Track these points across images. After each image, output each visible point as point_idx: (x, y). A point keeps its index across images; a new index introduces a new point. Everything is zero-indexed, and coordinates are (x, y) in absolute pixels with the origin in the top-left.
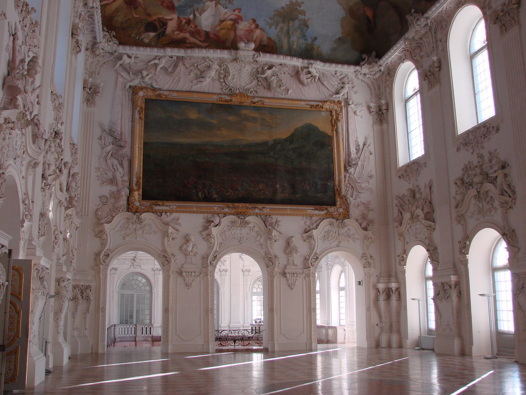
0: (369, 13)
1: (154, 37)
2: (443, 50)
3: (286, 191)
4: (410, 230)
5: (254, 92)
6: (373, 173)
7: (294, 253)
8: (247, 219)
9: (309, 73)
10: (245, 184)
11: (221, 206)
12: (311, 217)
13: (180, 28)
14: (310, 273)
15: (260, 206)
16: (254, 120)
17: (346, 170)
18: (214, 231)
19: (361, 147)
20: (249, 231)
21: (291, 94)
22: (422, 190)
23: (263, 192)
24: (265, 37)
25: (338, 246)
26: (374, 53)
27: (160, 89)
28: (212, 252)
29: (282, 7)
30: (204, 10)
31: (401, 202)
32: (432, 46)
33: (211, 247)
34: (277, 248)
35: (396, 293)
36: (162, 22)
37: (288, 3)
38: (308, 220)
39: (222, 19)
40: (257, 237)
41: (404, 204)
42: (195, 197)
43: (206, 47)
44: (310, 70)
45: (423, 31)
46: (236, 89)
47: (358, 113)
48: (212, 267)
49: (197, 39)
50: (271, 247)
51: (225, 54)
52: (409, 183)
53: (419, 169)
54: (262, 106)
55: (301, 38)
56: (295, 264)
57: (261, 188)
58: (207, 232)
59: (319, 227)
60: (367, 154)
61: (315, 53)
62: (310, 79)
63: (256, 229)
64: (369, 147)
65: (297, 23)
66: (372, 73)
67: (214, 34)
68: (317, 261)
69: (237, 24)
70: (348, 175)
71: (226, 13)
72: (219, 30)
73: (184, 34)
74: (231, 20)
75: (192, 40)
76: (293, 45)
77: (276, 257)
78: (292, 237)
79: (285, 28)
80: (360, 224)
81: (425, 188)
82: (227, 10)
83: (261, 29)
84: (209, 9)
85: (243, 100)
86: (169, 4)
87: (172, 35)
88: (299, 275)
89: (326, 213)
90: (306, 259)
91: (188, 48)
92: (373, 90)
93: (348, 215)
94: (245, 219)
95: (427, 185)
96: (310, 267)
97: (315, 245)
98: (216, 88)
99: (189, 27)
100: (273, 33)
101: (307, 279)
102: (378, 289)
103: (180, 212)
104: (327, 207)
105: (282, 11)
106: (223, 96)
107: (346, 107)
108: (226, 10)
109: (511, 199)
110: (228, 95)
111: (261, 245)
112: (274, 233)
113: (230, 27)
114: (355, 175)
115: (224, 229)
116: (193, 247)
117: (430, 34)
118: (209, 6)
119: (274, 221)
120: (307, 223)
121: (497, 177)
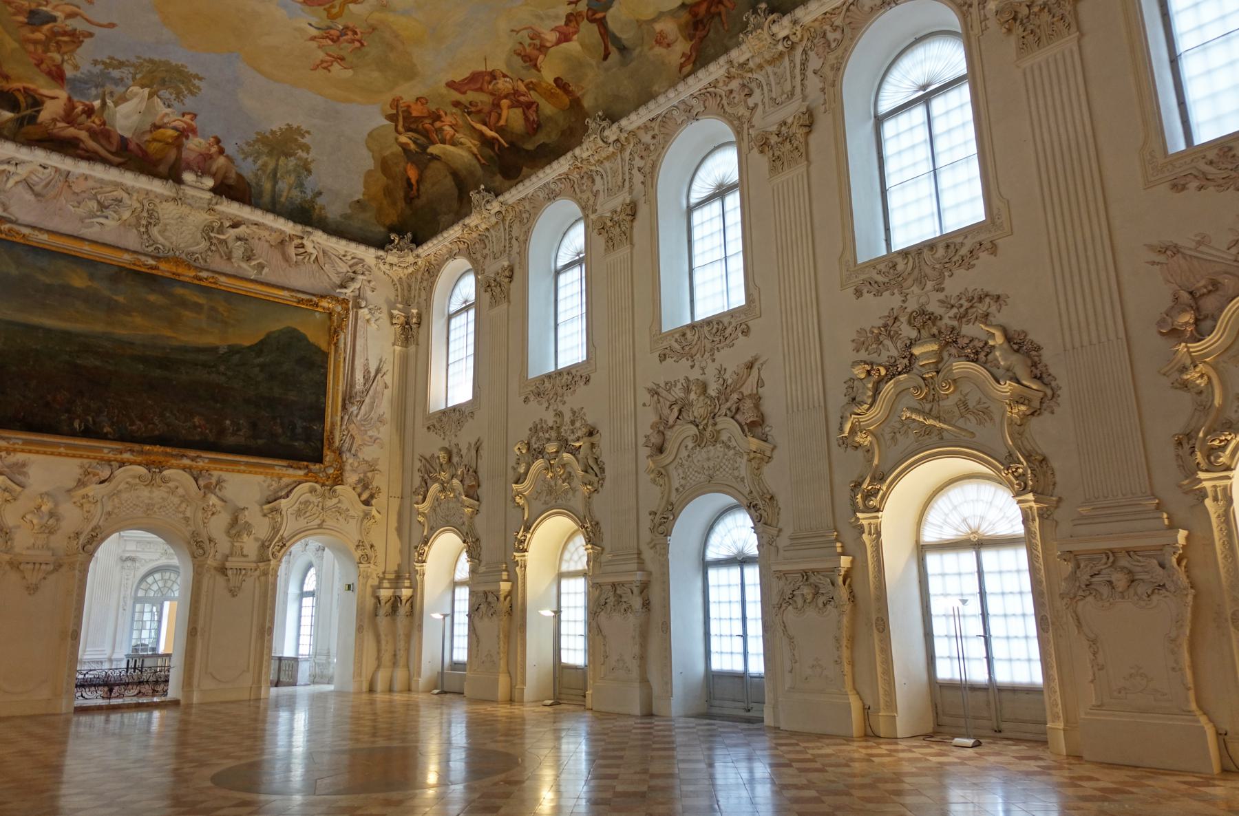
0: (413, 174)
1: (10, 120)
2: (519, 253)
3: (241, 433)
4: (438, 509)
5: (201, 260)
6: (388, 416)
7: (245, 535)
8: (166, 473)
9: (303, 246)
10: (168, 415)
13: (69, 117)
14: (268, 569)
15: (192, 453)
16: (197, 307)
17: (344, 407)
19: (373, 374)
20: (165, 495)
21: (266, 275)
22: (464, 452)
23: (199, 430)
24: (234, 171)
25: (320, 526)
26: (409, 235)
27: (11, 222)
29: (272, 130)
30: (123, 99)
31: (428, 465)
32: (503, 244)
33: (87, 520)
34: (217, 526)
35: (408, 604)
36: (33, 98)
37: (284, 127)
39: (157, 124)
40: (179, 505)
41: (432, 470)
42: (65, 428)
43: (118, 165)
44: (305, 242)
45: (494, 220)
46: (169, 250)
47: (372, 322)
48: (85, 555)
49: (102, 146)
50: (205, 523)
51: (157, 187)
52: (444, 439)
53: (462, 419)
54: (214, 286)
55: (296, 188)
56: (245, 553)
57: (197, 424)
59: (290, 497)
60: (381, 385)
61: (315, 216)
62: (302, 257)
64: (385, 377)
65: (292, 162)
66: (403, 265)
67: (138, 145)
68: (283, 550)
69: (184, 139)
70: (346, 417)
71: (167, 114)
72: (149, 141)
73: (76, 131)
74: (175, 128)
75: (92, 144)
76: (281, 196)
77: (210, 540)
78: (244, 509)
79: (271, 166)
80: (360, 495)
81: (469, 449)
82: (169, 109)
83: (227, 157)
84: (135, 101)
85: (180, 271)
86: (54, 68)
87: (51, 127)
88: (249, 572)
89: (306, 475)
90: (264, 546)
91: (82, 158)
92: (399, 289)
93: (342, 480)
94: (160, 472)
95: (473, 445)
96: (269, 560)
97: (281, 524)
98: (132, 240)
99: (89, 120)
100: (248, 169)
101: (263, 578)
102: (378, 599)
103: (30, 452)
104: (309, 464)
105: (271, 137)
106: (143, 258)
107: (355, 310)
108: (168, 110)
109: (597, 479)
110: (153, 257)
111: (187, 519)
113: (170, 141)
114: (359, 418)
115: (119, 488)
117: (502, 225)
118: (136, 95)
119: (214, 480)
120: (271, 488)
121: (580, 446)
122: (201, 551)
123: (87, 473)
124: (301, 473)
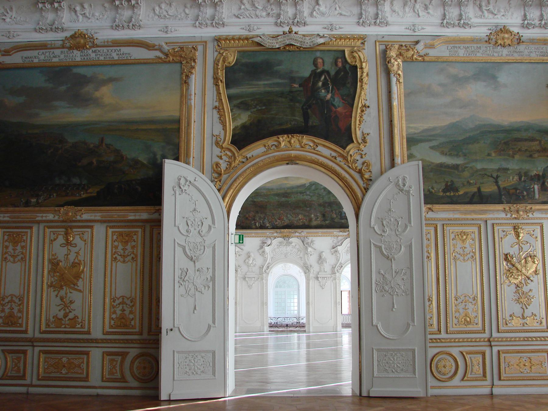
3: (319, 219)
8: (290, 240)
11: (272, 231)
12: (338, 237)
14: (336, 277)
18: (267, 249)
20: (292, 249)
28: (266, 264)
33: (265, 260)
38: (335, 239)
42: (254, 226)
56: (325, 271)
58: (262, 250)
59: (343, 245)
63: (297, 247)
88: (328, 279)
90: (333, 268)
101: (334, 281)
111: (301, 257)
112: (310, 249)
116: (253, 261)
119: (309, 241)
120: (334, 242)
122: (308, 271)
123: (264, 243)
124: (346, 234)
